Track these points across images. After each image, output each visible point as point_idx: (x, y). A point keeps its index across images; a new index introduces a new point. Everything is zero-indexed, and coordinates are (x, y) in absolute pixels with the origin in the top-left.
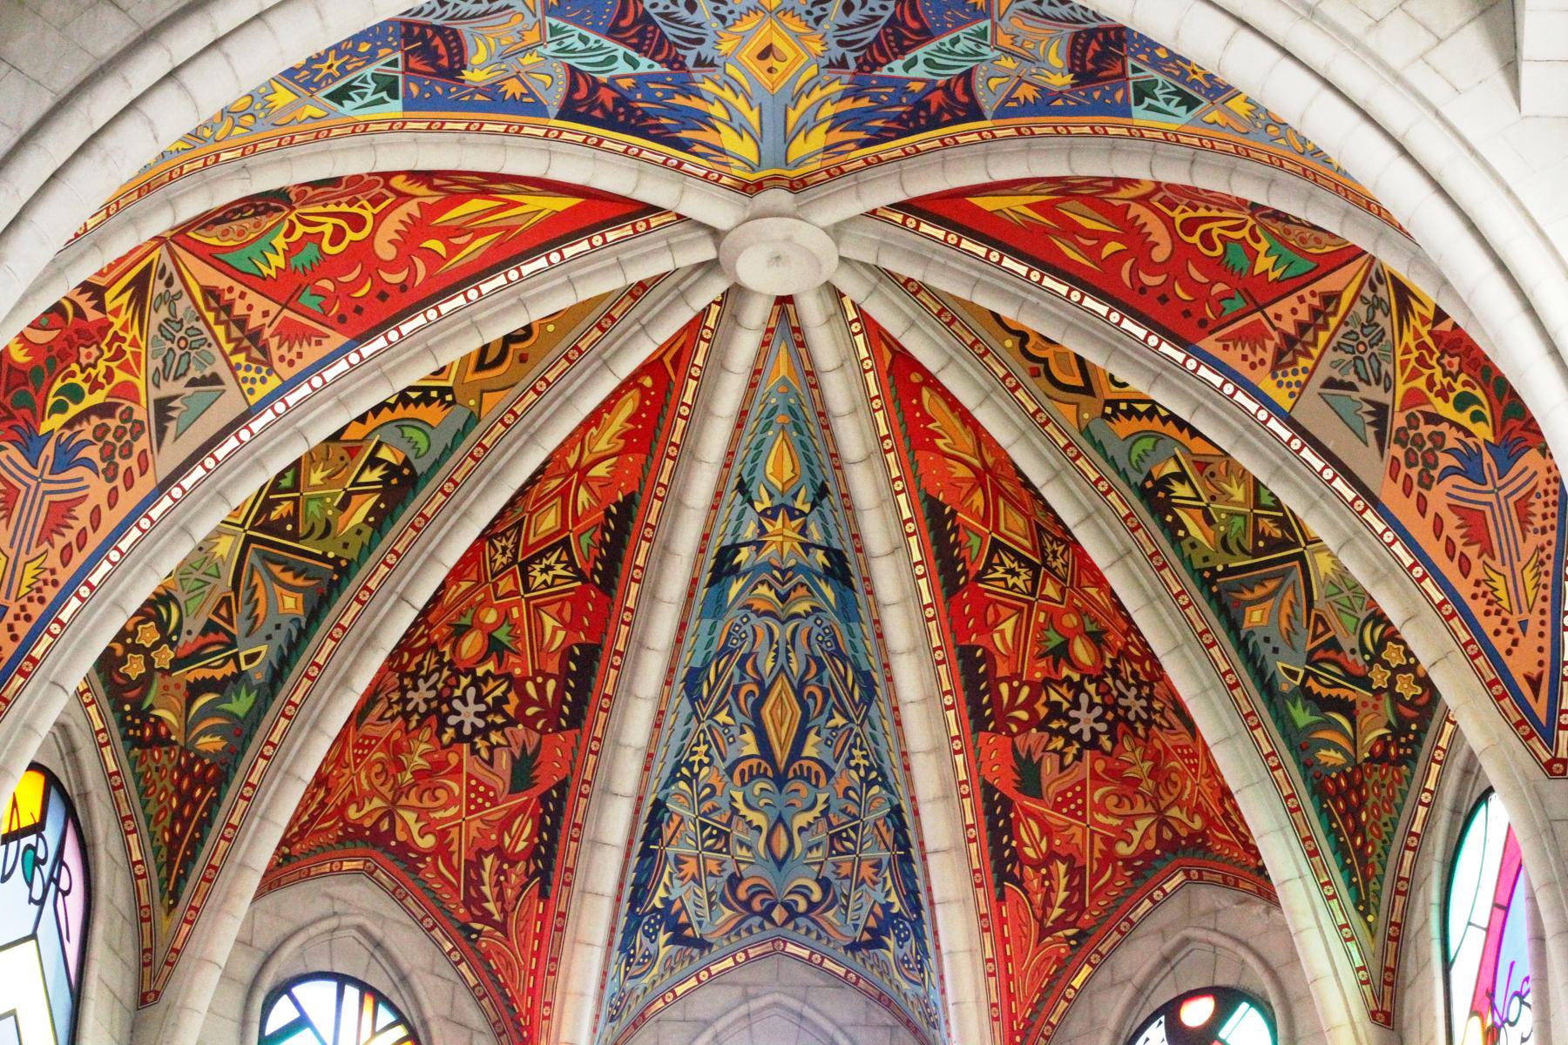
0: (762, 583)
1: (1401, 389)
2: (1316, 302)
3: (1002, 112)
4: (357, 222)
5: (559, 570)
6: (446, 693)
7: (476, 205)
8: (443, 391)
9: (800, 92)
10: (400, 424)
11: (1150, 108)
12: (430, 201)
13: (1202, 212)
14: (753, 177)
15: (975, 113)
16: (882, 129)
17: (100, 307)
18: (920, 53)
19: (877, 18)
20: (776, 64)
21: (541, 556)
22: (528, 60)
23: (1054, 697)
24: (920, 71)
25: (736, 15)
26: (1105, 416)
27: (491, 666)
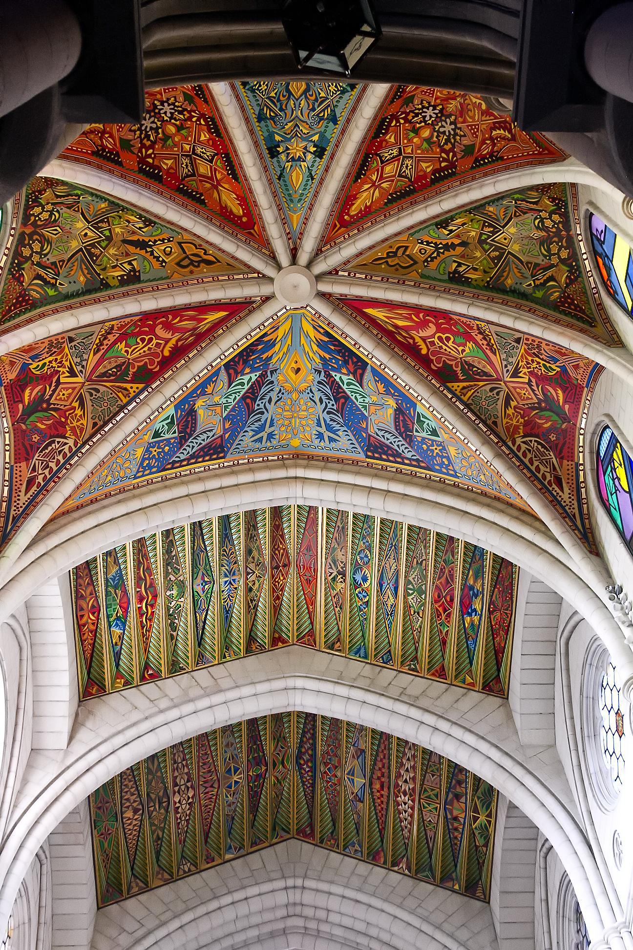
0: (304, 134)
1: (66, 350)
2: (101, 348)
3: (217, 373)
4: (440, 338)
5: (386, 155)
6: (438, 120)
7: (400, 323)
8: (422, 243)
9: (286, 354)
10: (439, 238)
11: (167, 418)
12: (414, 332)
13: (146, 349)
14: (303, 311)
15: (227, 366)
16: (258, 345)
17: (530, 380)
18: (246, 387)
19: (261, 399)
20: (293, 365)
21: (393, 157)
22: (374, 398)
23: (182, 116)
24: (247, 378)
25: (307, 391)
26: (173, 237)
27: (418, 125)
